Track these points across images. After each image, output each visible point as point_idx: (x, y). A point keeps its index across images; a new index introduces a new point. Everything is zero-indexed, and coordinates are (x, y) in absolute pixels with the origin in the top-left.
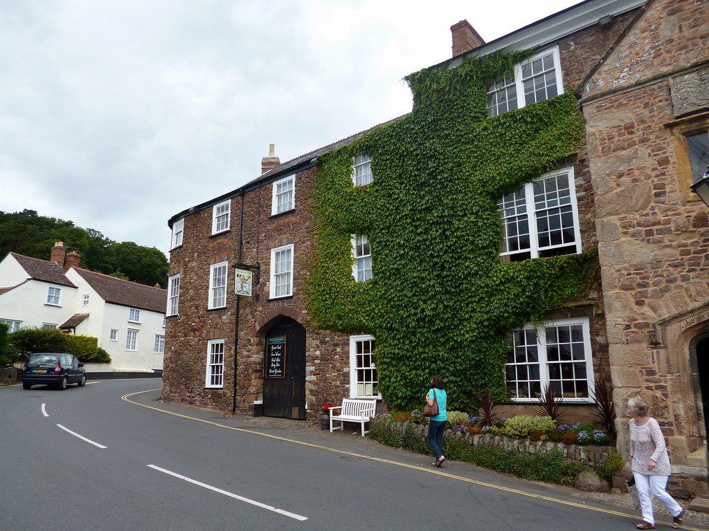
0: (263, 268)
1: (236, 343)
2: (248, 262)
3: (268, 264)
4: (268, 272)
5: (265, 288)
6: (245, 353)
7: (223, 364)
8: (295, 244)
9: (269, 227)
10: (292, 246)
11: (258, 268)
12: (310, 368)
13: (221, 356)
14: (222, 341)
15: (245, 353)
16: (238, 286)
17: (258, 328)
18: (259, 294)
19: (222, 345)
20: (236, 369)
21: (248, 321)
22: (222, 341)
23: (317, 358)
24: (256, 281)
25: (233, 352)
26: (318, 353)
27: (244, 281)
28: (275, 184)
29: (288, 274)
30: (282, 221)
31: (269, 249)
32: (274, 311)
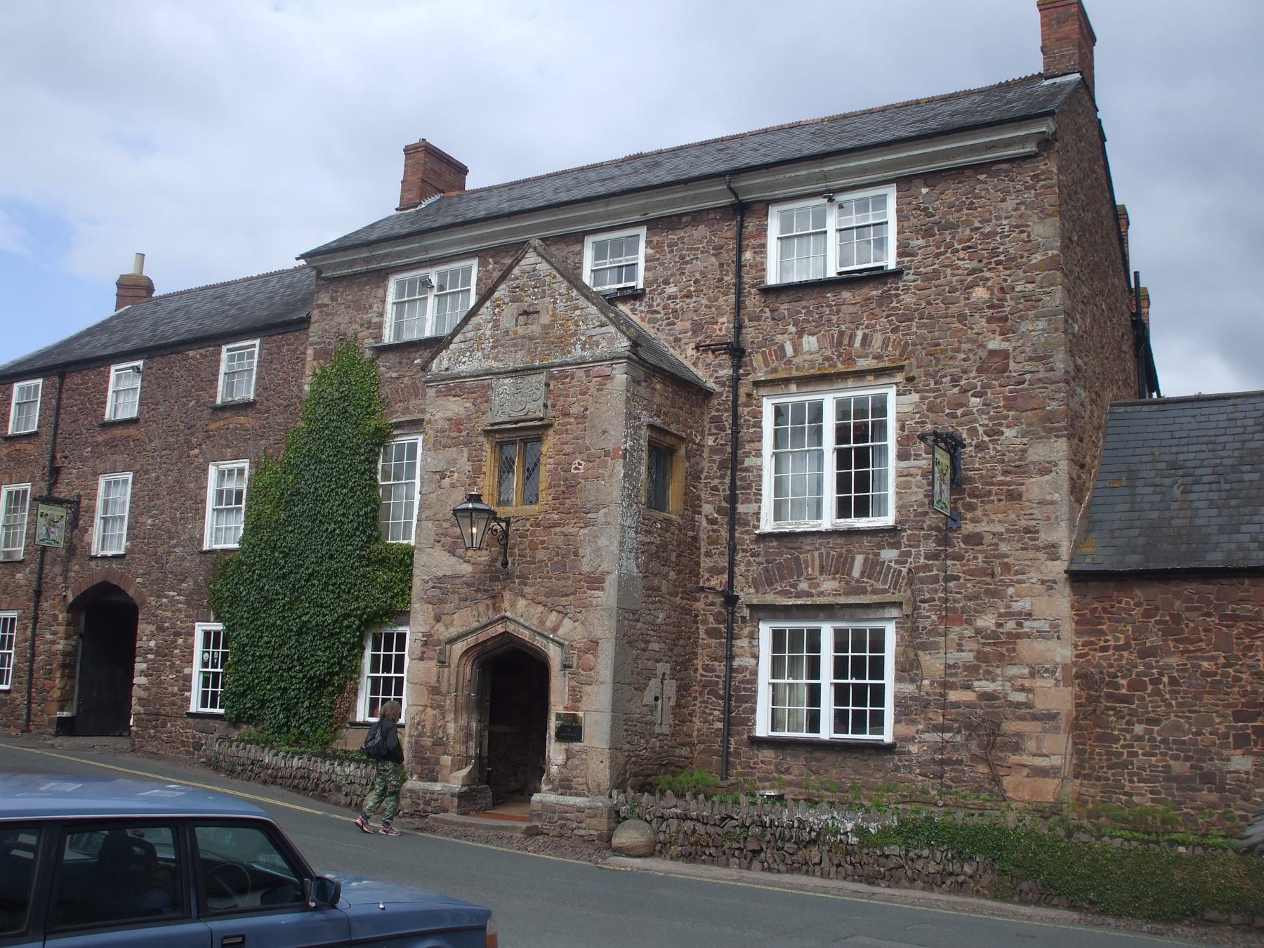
0: (84, 503)
1: (36, 619)
2: (63, 491)
3: (94, 498)
4: (91, 510)
5: (86, 537)
6: (49, 637)
7: (12, 651)
8: (135, 473)
9: (99, 439)
10: (130, 476)
11: (78, 503)
12: (140, 666)
13: (11, 637)
14: (14, 614)
15: (49, 637)
16: (42, 531)
17: (70, 599)
18: (75, 547)
19: (13, 620)
20: (32, 661)
21: (56, 586)
22: (14, 614)
23: (150, 651)
24: (74, 524)
25: (29, 633)
26: (152, 644)
27: (52, 523)
28: (113, 368)
29: (122, 518)
30: (118, 432)
31: (96, 474)
32: (97, 573)
